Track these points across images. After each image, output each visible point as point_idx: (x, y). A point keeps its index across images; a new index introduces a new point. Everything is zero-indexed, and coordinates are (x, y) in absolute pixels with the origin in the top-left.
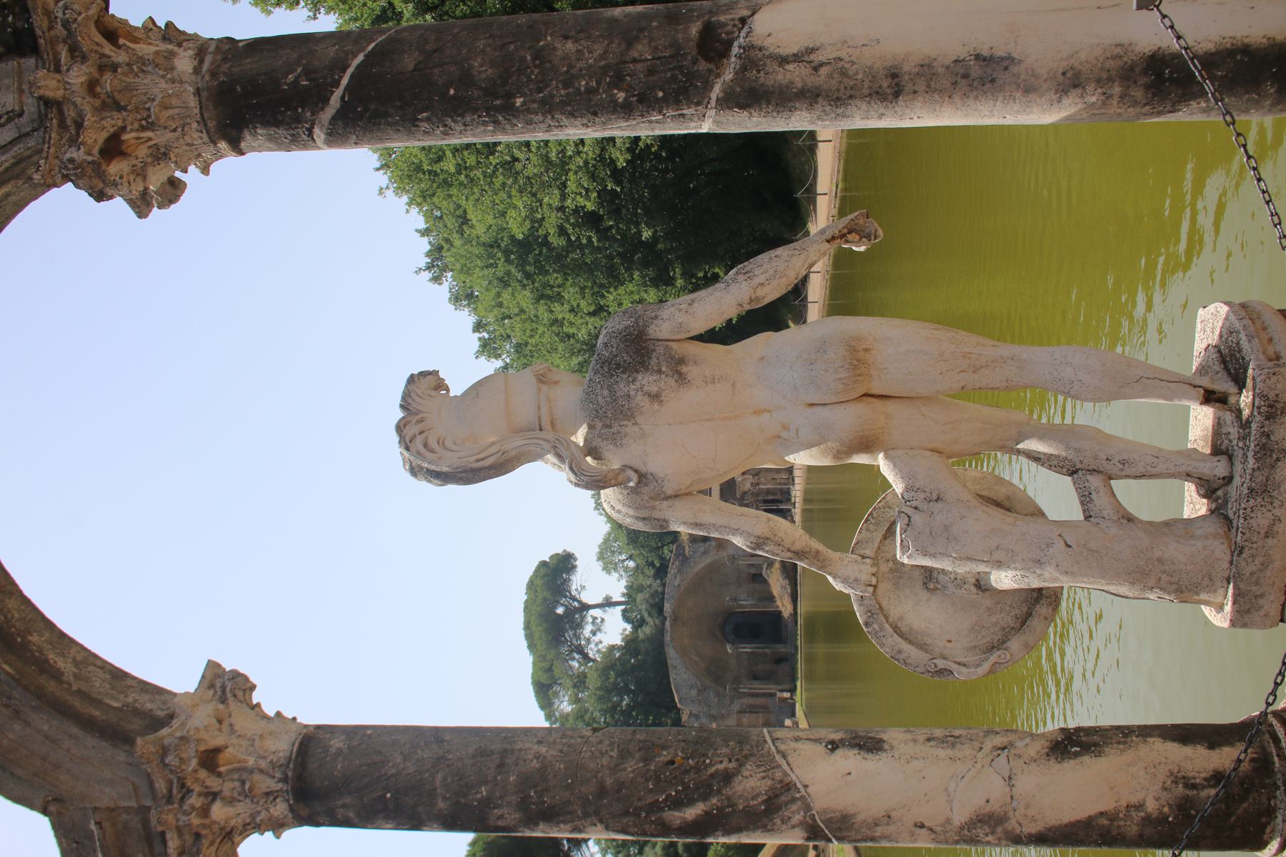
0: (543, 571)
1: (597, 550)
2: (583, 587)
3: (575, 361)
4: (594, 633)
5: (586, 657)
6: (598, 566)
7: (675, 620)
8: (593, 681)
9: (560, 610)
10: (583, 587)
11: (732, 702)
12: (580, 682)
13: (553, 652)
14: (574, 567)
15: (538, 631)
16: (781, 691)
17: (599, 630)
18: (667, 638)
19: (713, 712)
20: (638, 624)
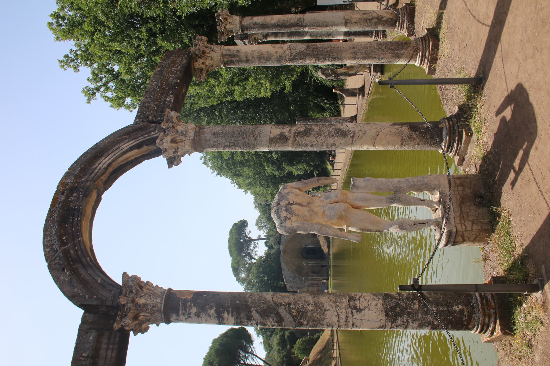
0: (235, 227)
1: (256, 222)
2: (250, 232)
3: (248, 181)
4: (254, 248)
5: (251, 258)
6: (256, 228)
7: (284, 252)
8: (254, 270)
9: (242, 240)
10: (250, 232)
11: (305, 282)
12: (249, 270)
13: (239, 257)
14: (247, 226)
15: (233, 250)
16: (323, 279)
17: (256, 247)
18: (282, 259)
19: (298, 286)
20: (270, 247)
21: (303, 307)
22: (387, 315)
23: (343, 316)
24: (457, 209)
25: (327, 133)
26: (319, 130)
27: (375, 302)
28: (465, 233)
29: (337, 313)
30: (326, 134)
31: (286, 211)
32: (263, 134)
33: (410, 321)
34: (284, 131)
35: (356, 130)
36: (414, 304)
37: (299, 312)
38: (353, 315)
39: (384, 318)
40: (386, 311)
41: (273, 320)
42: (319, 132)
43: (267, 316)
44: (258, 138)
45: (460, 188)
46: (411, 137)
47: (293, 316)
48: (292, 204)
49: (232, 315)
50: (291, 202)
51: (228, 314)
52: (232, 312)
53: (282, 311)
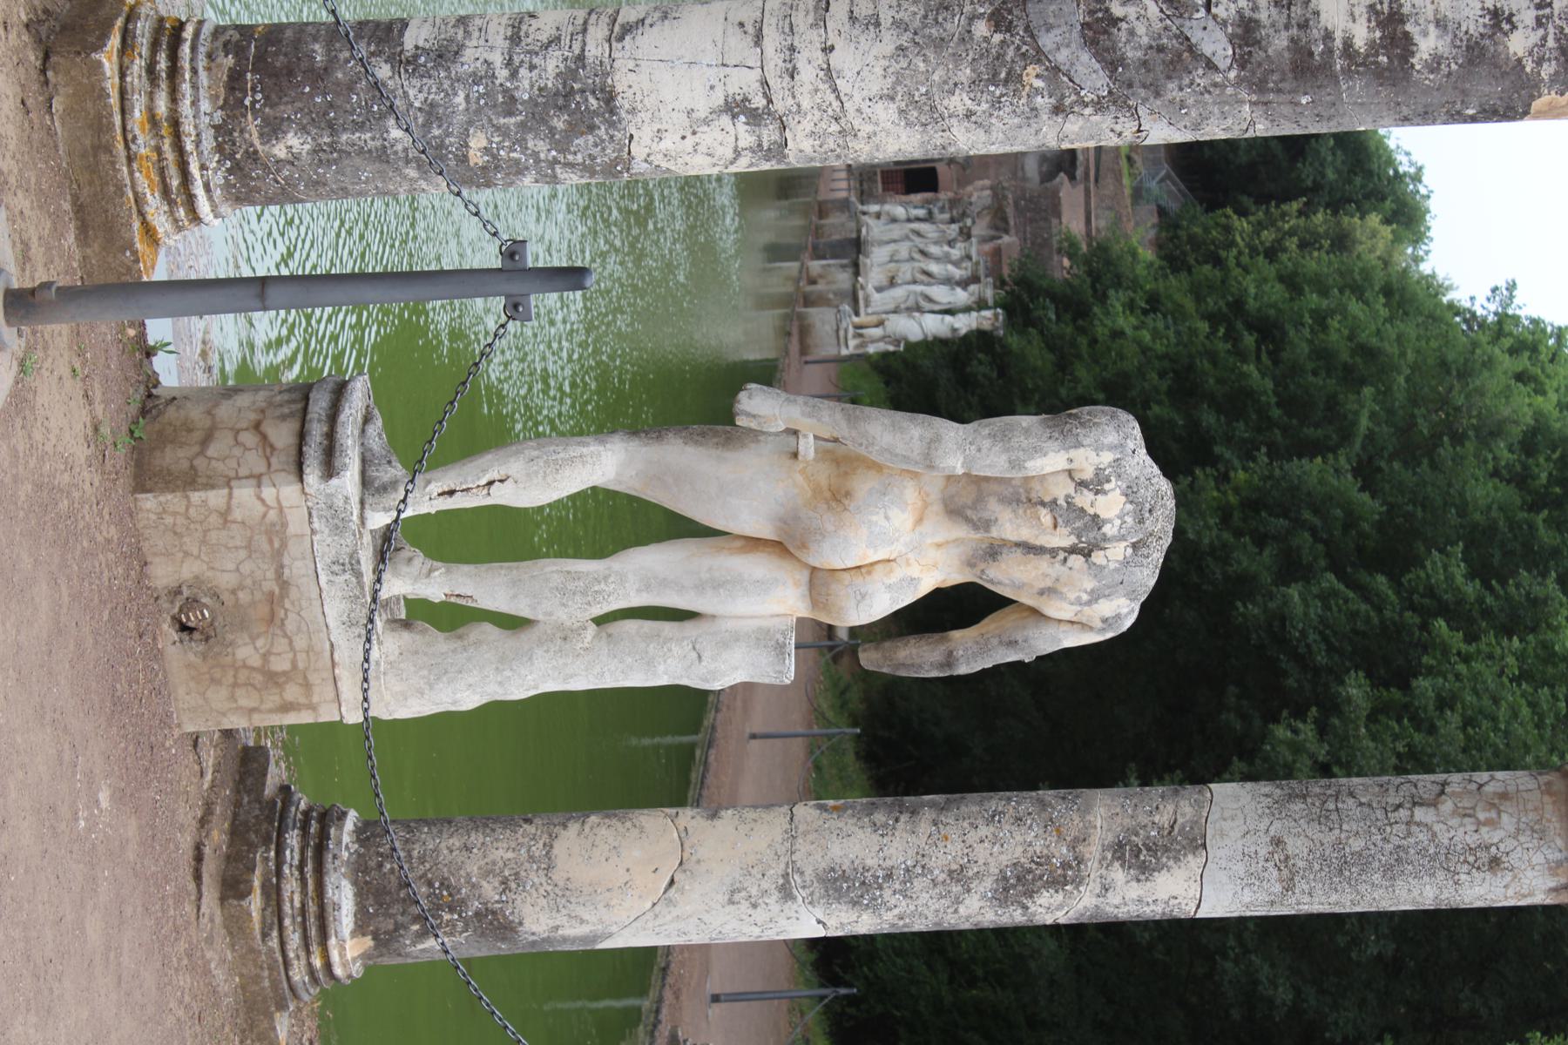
21: (996, 103)
22: (609, 97)
23: (808, 73)
24: (297, 568)
25: (919, 884)
26: (958, 901)
27: (666, 144)
28: (261, 467)
29: (835, 90)
30: (926, 881)
31: (1096, 521)
32: (1240, 868)
33: (502, 74)
34: (1134, 891)
35: (775, 908)
36: (487, 150)
37: (1014, 79)
38: (765, 83)
39: (621, 81)
40: (612, 112)
41: (1132, 32)
42: (956, 889)
43: (1161, 49)
44: (1263, 852)
45: (280, 664)
46: (504, 882)
47: (1039, 56)
48: (1072, 550)
49: (1328, 36)
50: (1076, 561)
51: (1348, 43)
52: (1329, 51)
53: (1092, 77)
